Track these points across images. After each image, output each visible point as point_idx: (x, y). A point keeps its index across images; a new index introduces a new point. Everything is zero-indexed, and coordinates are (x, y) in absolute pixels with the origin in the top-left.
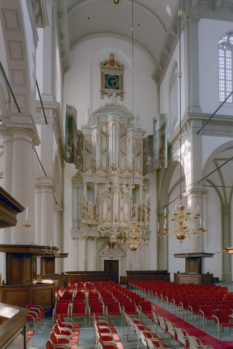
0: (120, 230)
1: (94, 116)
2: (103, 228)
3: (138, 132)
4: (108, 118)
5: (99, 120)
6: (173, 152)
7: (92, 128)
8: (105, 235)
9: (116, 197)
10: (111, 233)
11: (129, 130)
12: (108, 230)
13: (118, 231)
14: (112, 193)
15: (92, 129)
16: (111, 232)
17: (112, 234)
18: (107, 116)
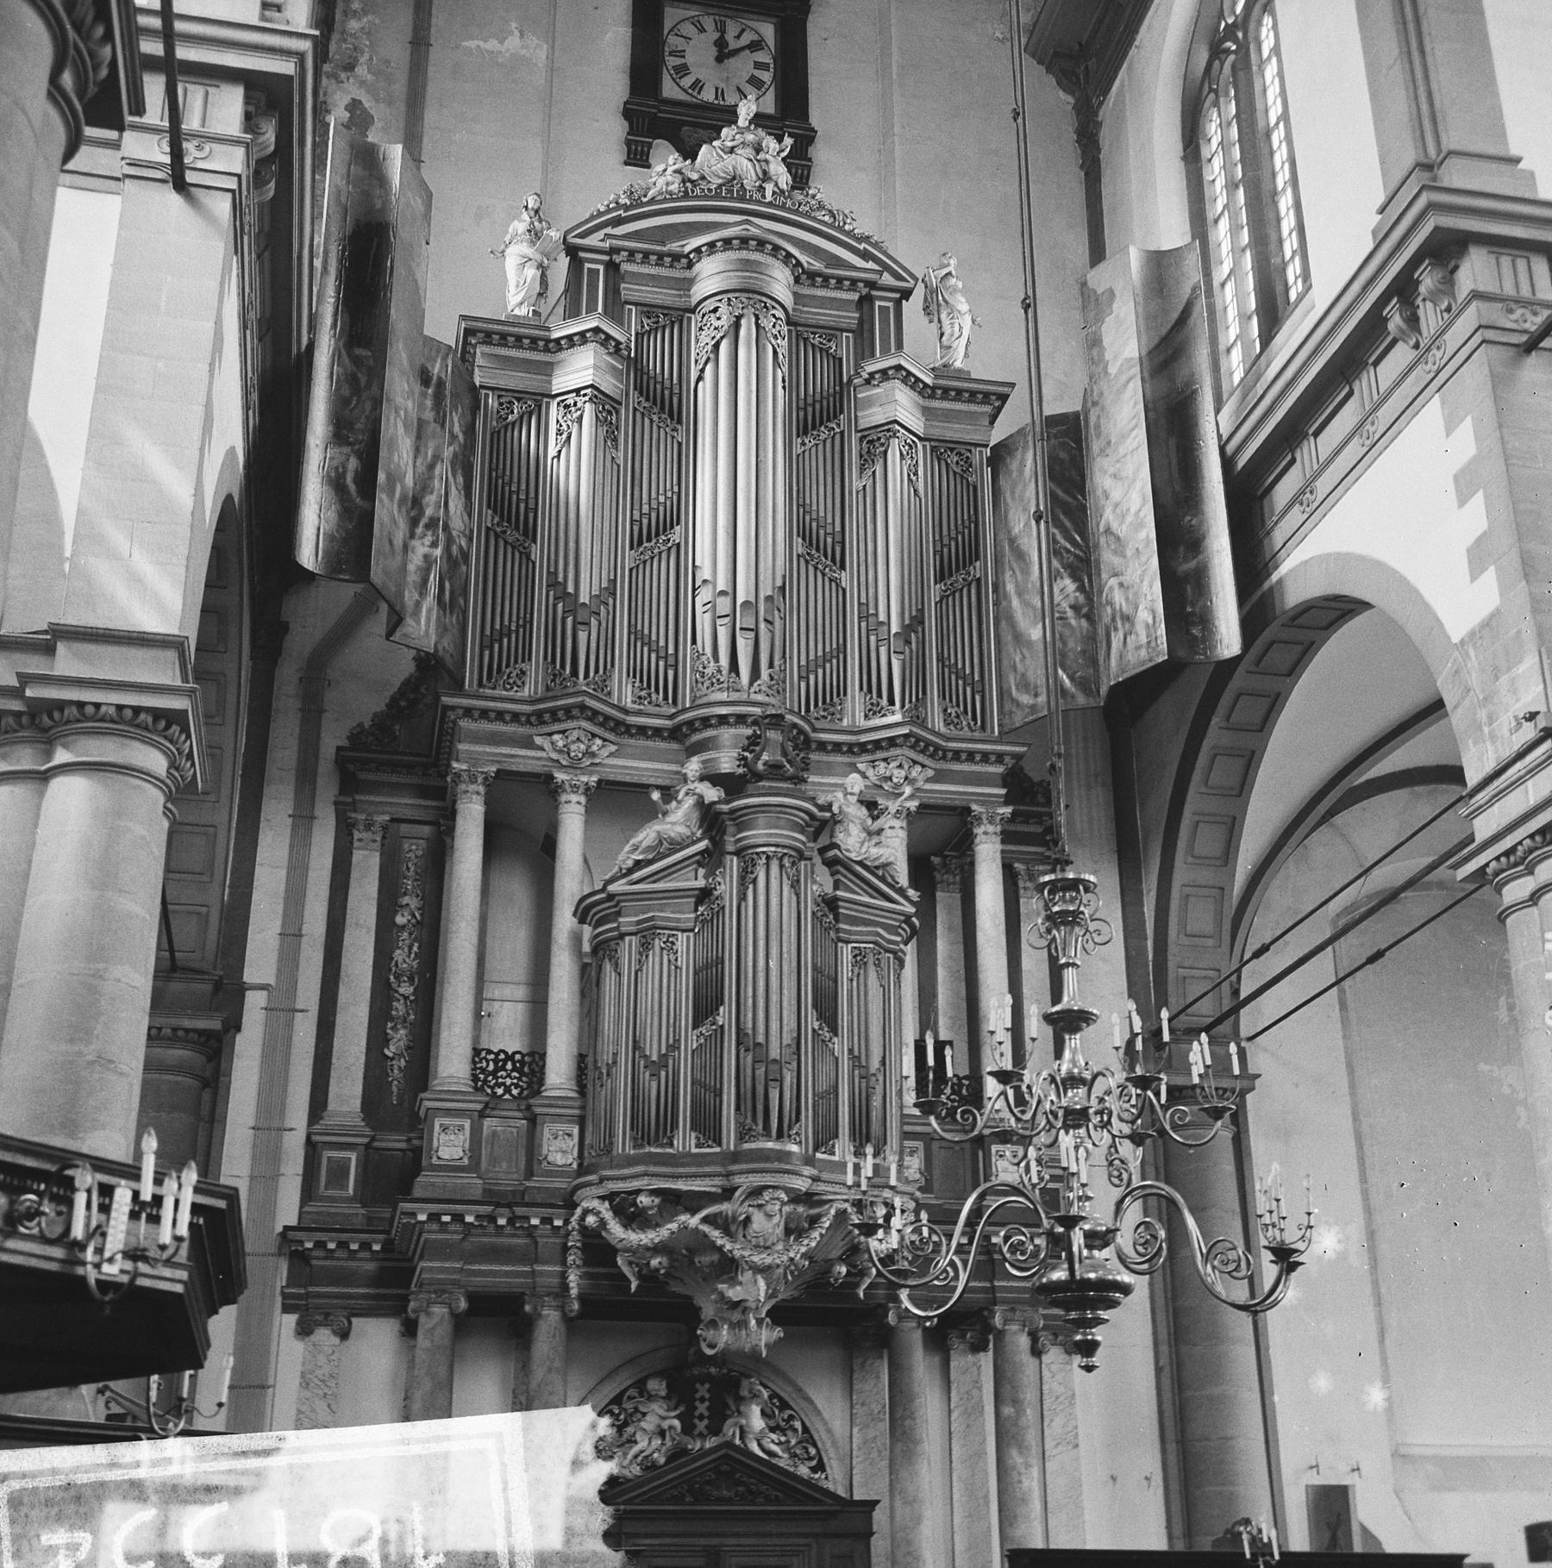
0: (814, 1221)
1: (572, 251)
2: (638, 1192)
3: (946, 390)
4: (691, 282)
5: (613, 292)
6: (1278, 536)
7: (558, 341)
8: (648, 1277)
9: (774, 901)
10: (720, 1249)
11: (871, 368)
12: (694, 1221)
13: (788, 1231)
14: (733, 863)
15: (557, 345)
16: (715, 1234)
17: (729, 1267)
18: (690, 266)
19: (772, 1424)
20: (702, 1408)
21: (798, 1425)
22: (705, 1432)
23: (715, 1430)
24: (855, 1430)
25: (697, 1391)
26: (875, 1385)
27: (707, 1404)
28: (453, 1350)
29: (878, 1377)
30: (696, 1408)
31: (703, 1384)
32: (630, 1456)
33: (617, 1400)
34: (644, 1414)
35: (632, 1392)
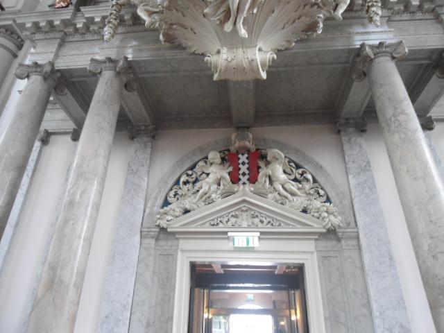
19: (293, 177)
20: (244, 169)
21: (309, 177)
22: (247, 182)
23: (253, 180)
24: (350, 177)
25: (239, 159)
26: (360, 151)
27: (247, 166)
28: (109, 154)
29: (361, 147)
30: (240, 169)
31: (243, 154)
32: (197, 197)
33: (192, 168)
34: (208, 174)
35: (201, 163)
